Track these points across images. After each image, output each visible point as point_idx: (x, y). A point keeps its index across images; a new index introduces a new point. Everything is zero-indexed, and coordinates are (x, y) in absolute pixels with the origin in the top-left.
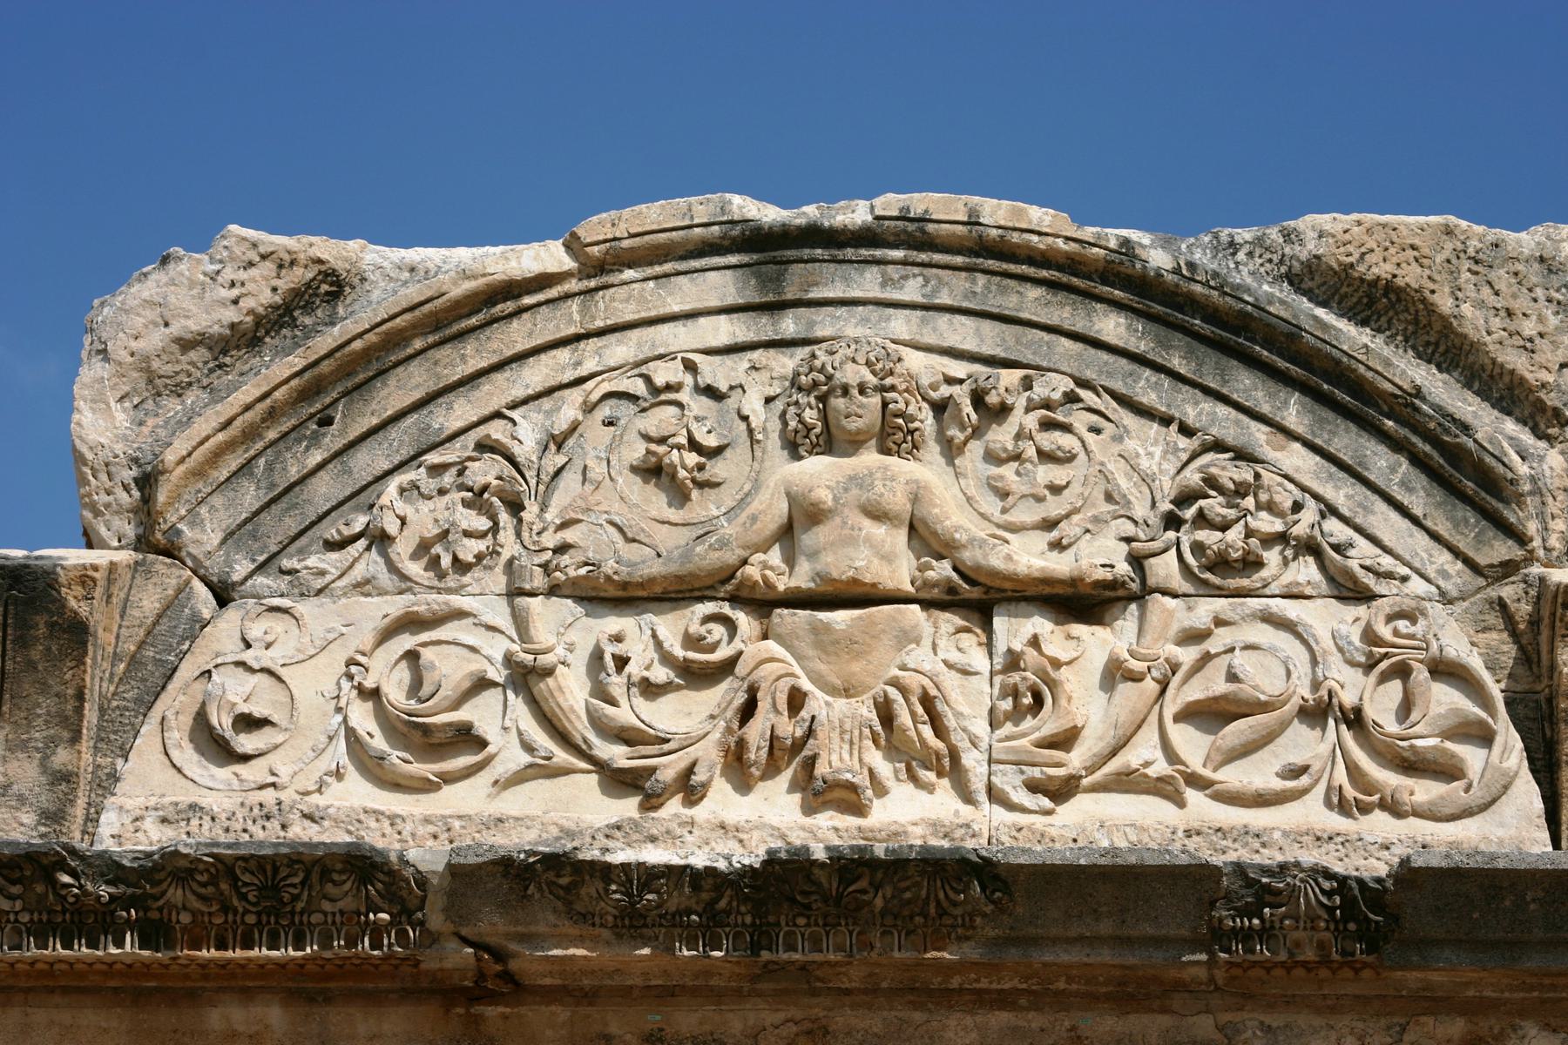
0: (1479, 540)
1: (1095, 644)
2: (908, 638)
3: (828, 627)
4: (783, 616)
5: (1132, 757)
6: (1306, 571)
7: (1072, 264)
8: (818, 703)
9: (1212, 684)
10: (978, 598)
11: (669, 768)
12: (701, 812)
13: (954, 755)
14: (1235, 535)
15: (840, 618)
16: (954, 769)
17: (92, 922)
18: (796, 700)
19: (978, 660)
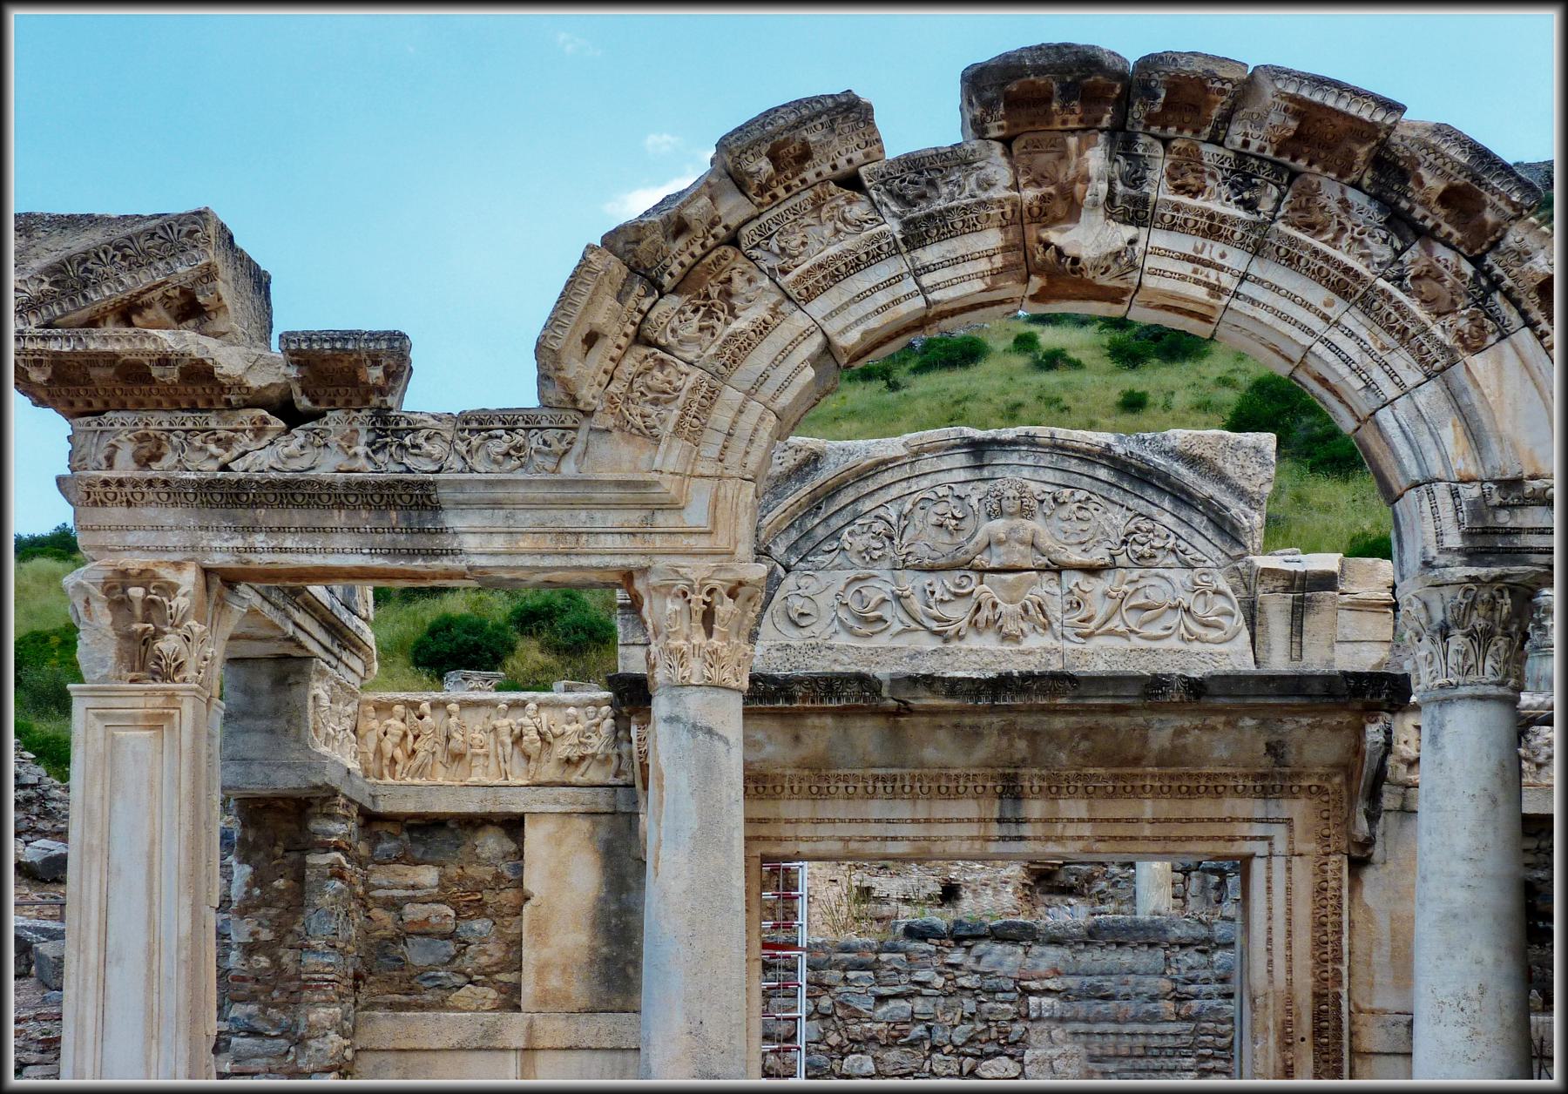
0: (1231, 548)
1: (1098, 585)
2: (1034, 583)
3: (1004, 581)
4: (987, 576)
5: (1109, 626)
6: (1171, 560)
7: (1088, 452)
8: (1002, 607)
9: (1140, 600)
10: (1057, 569)
11: (952, 630)
12: (963, 645)
13: (1050, 623)
14: (1146, 548)
15: (1010, 577)
16: (1047, 626)
17: (773, 698)
18: (995, 605)
19: (1057, 590)
